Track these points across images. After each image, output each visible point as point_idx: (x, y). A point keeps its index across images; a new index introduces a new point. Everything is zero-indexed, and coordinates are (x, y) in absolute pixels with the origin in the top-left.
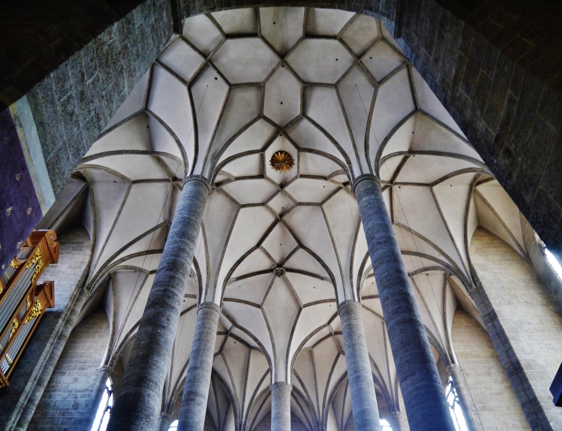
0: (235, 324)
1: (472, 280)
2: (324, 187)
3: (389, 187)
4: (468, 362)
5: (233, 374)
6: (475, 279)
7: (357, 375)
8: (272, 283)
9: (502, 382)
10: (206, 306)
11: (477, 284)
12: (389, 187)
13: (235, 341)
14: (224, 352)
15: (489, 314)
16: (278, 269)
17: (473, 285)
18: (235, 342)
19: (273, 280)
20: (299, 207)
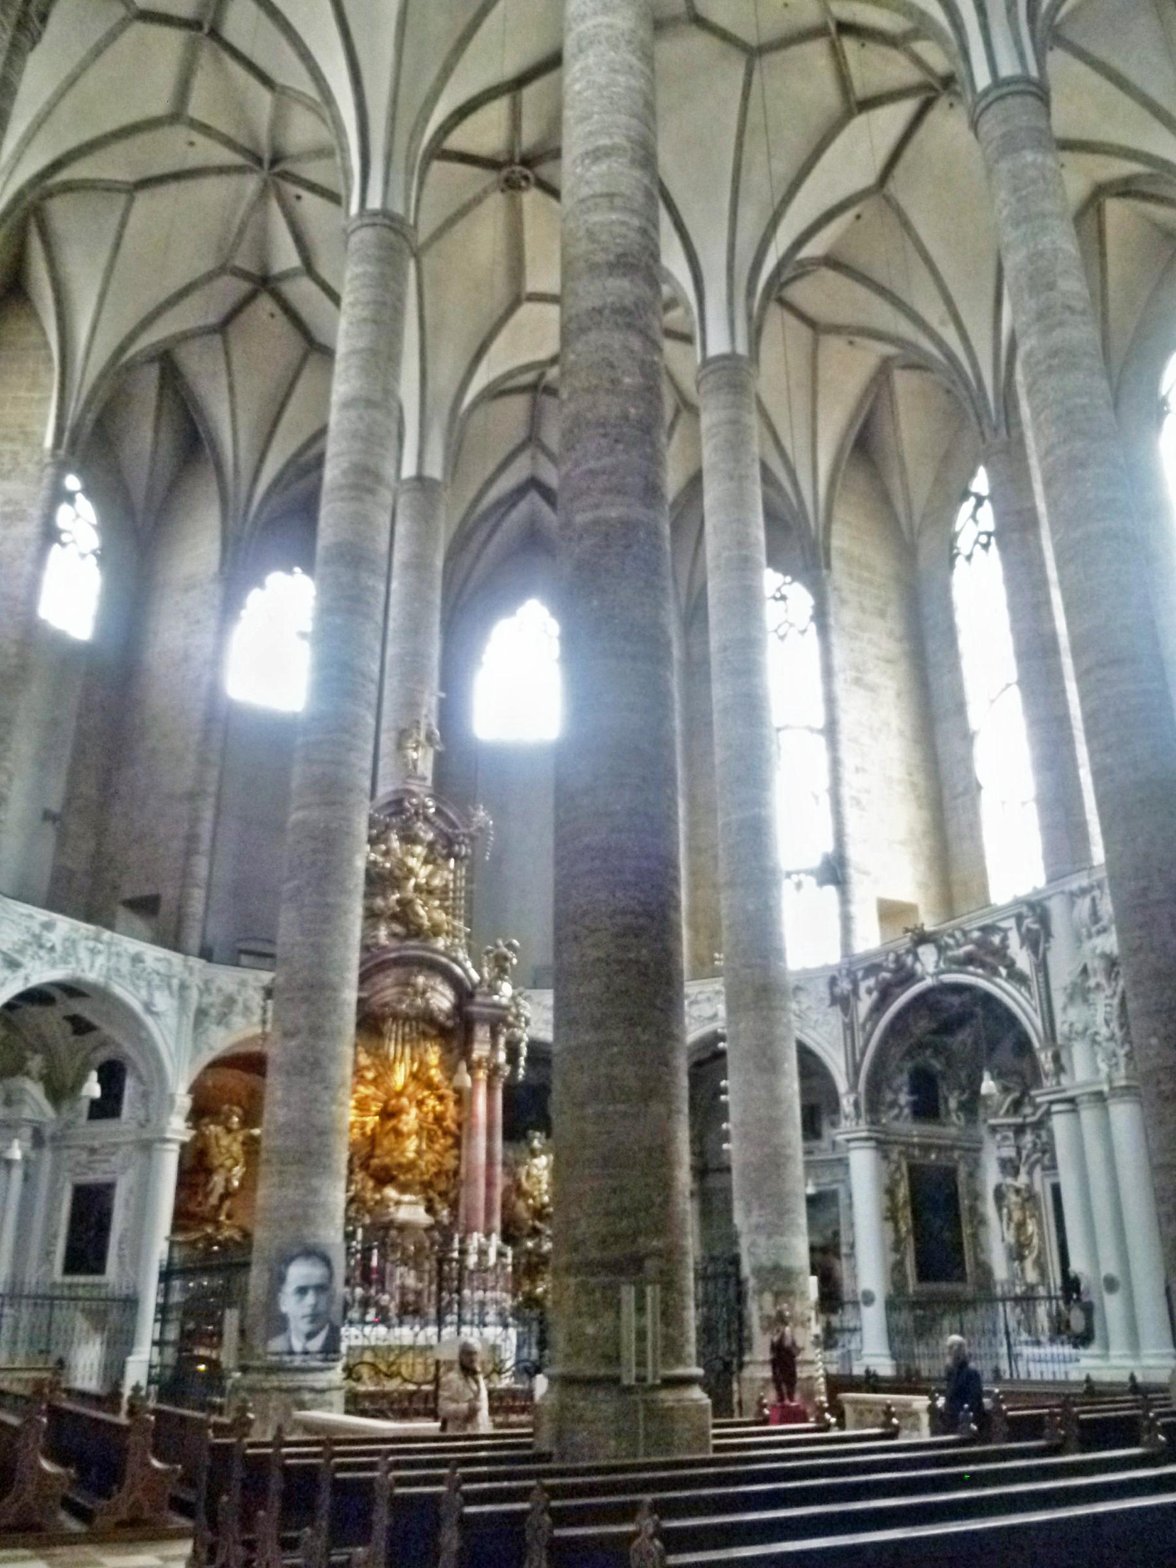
0: (309, 268)
1: (1002, 417)
2: (786, 5)
3: (932, 94)
4: (850, 575)
5: (240, 399)
6: (1012, 420)
7: (744, 552)
8: (477, 200)
9: (900, 640)
10: (387, 222)
11: (1014, 434)
12: (932, 94)
13: (277, 311)
14: (232, 330)
15: (1019, 513)
16: (518, 168)
17: (1003, 431)
18: (272, 316)
19: (486, 192)
20: (694, 28)
